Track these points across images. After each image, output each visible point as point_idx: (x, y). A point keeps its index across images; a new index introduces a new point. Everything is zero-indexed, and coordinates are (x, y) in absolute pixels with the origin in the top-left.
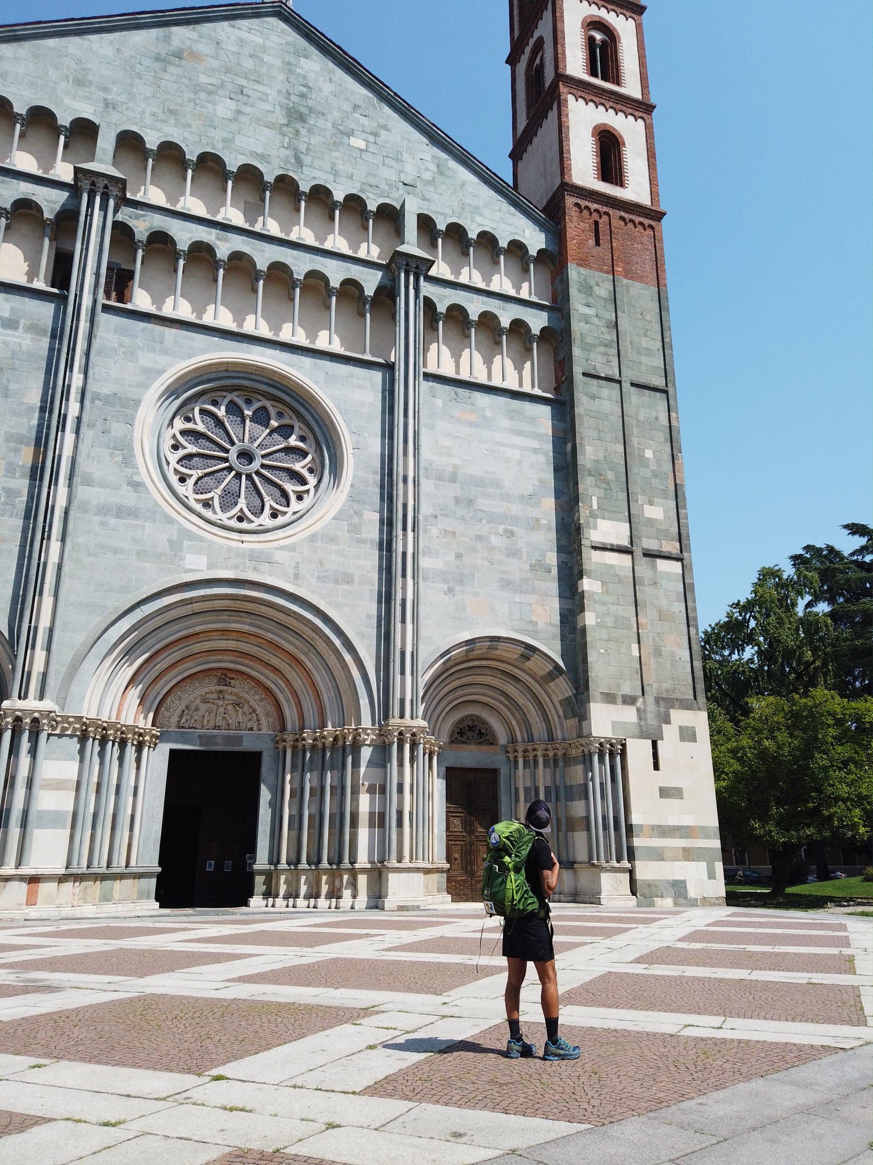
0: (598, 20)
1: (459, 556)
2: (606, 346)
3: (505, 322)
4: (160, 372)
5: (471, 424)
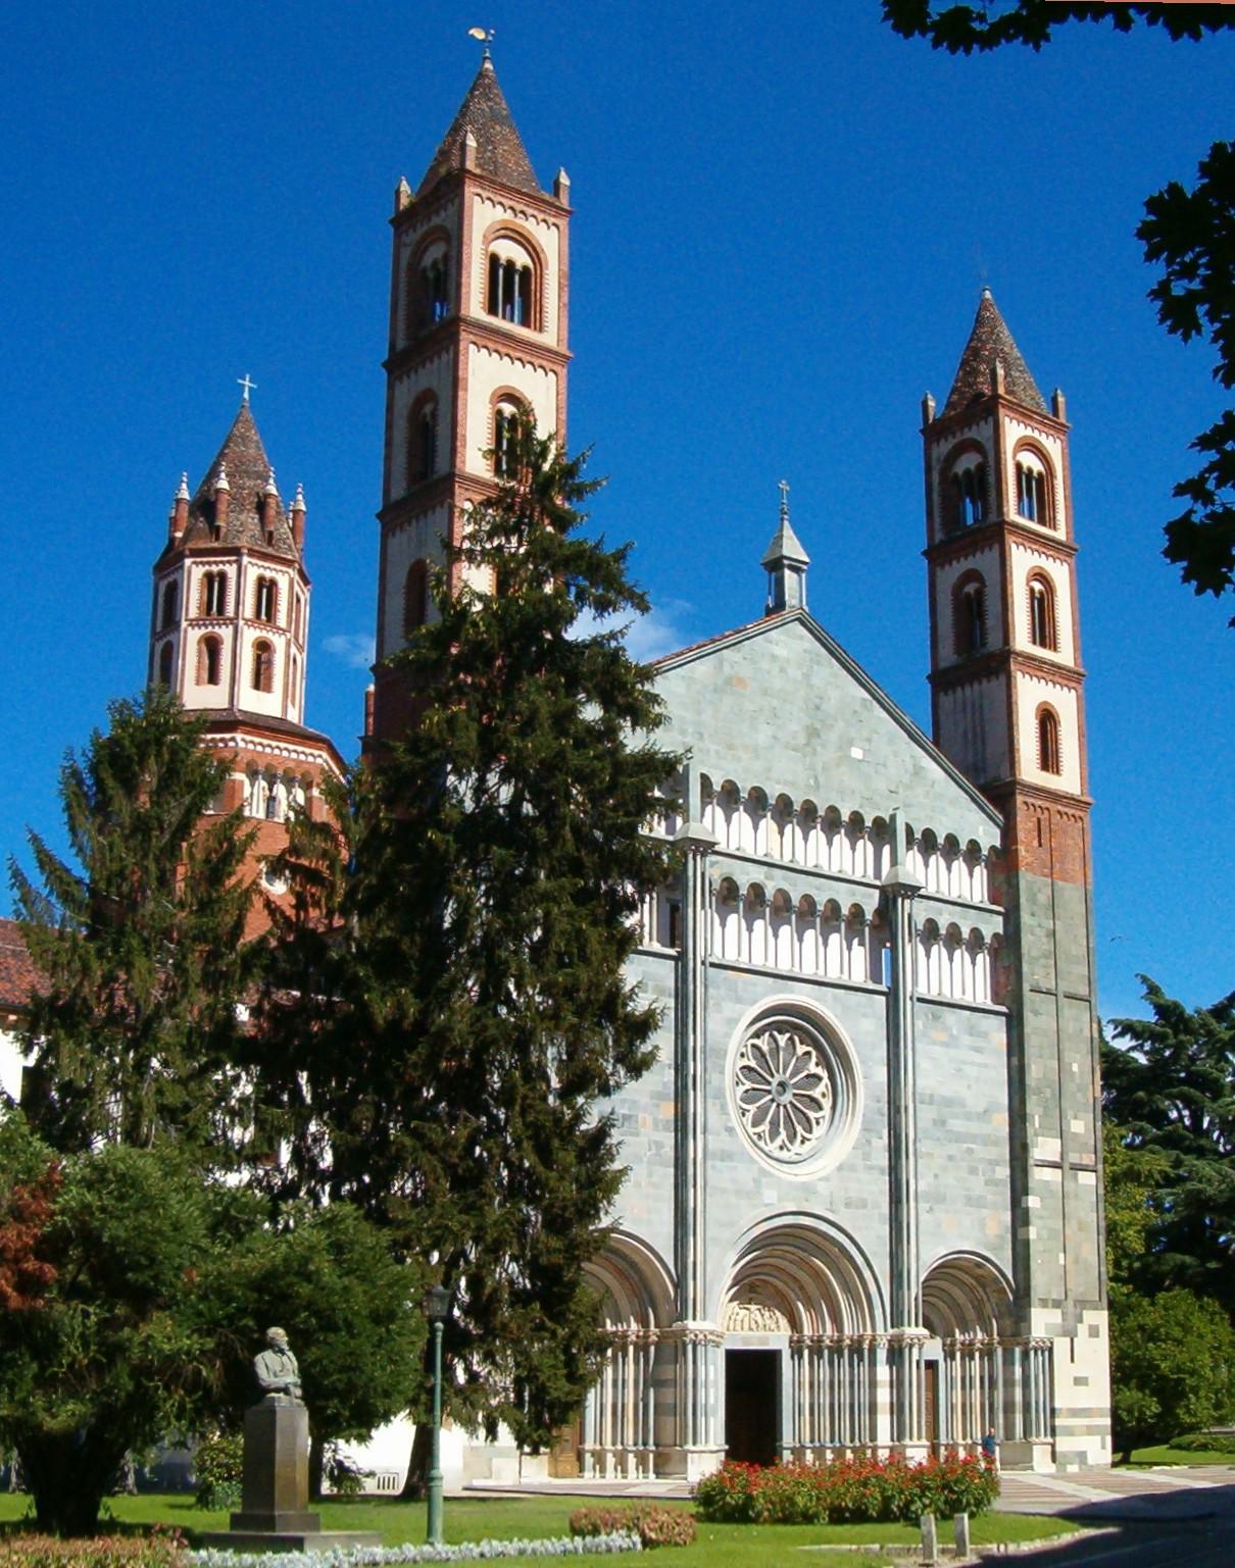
0: (1037, 571)
1: (936, 1176)
2: (1047, 957)
3: (966, 933)
4: (737, 1021)
5: (946, 1045)
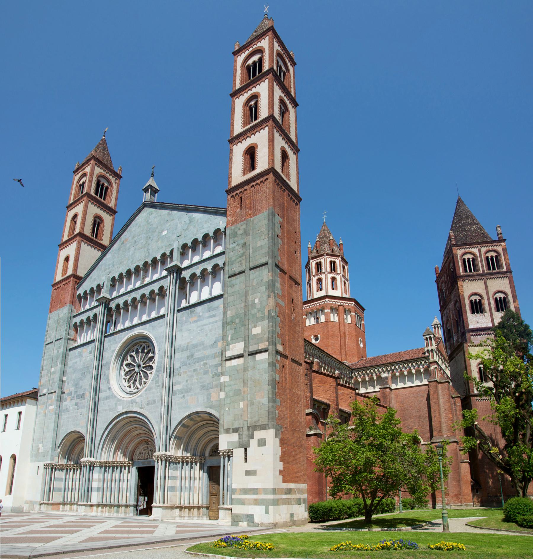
1: (187, 381)
